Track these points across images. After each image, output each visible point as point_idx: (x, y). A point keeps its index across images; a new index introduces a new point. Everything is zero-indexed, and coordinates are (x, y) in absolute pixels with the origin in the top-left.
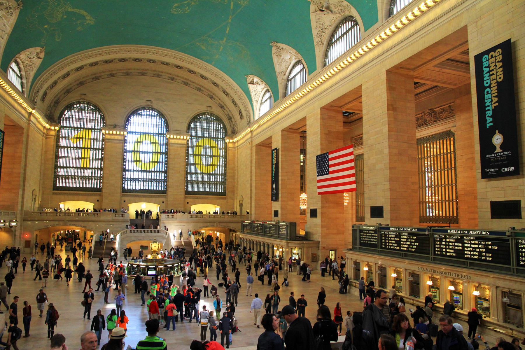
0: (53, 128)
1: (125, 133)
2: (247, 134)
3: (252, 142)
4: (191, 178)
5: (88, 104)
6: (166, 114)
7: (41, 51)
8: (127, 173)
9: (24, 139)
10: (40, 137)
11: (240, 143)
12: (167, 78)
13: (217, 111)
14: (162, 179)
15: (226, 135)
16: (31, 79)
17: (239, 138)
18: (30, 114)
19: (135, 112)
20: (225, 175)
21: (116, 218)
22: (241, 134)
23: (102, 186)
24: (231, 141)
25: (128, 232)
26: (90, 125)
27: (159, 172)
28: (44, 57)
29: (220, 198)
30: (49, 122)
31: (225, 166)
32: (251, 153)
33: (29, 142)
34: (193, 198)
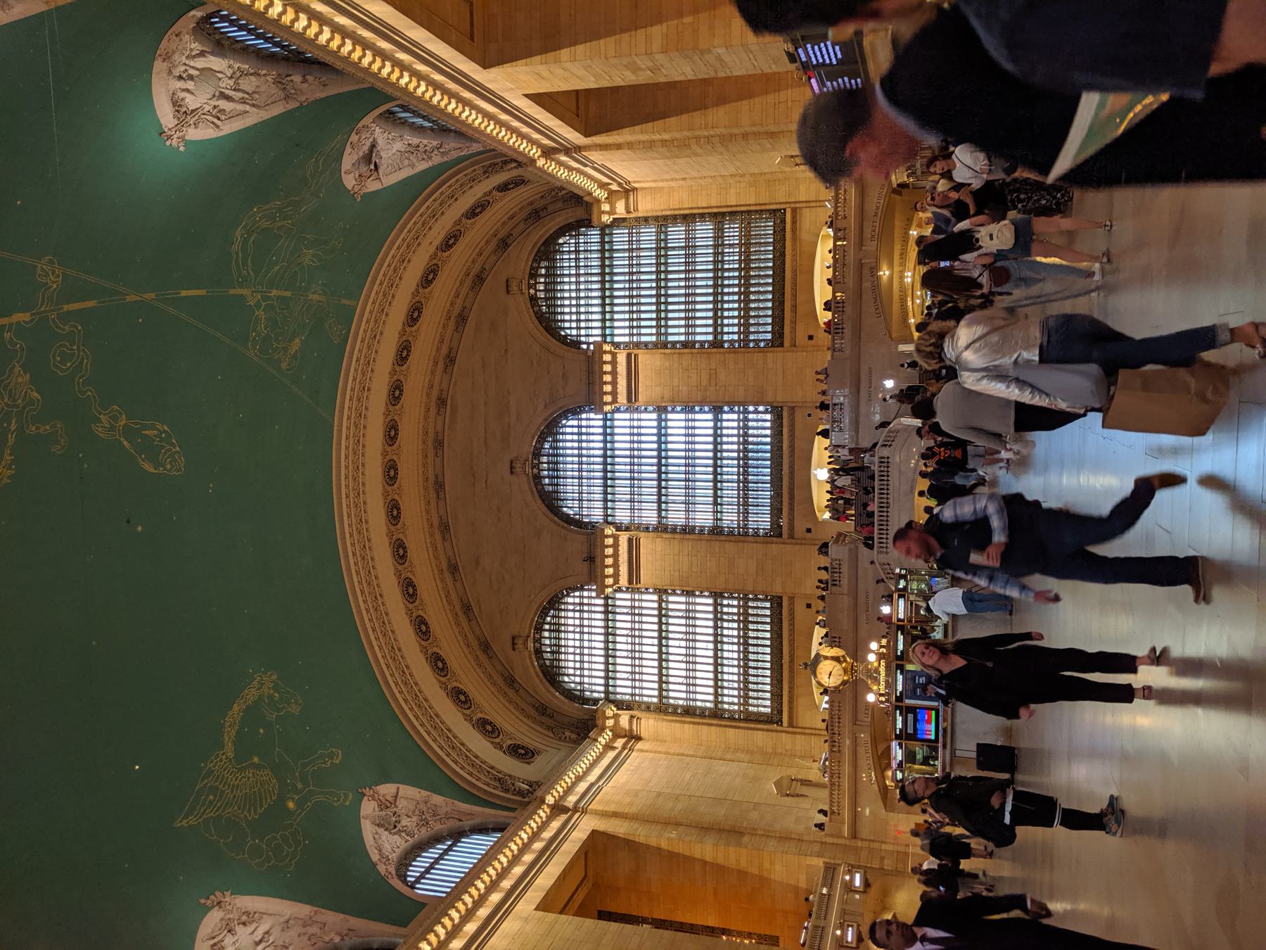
0: (610, 723)
1: (609, 531)
2: (560, 164)
3: (579, 149)
4: (731, 332)
6: (545, 415)
10: (634, 759)
11: (606, 180)
12: (440, 419)
13: (521, 256)
15: (588, 224)
18: (558, 809)
21: (845, 582)
22: (568, 182)
24: (606, 207)
29: (794, 230)
31: (688, 219)
32: (619, 147)
33: (633, 810)
34: (794, 322)
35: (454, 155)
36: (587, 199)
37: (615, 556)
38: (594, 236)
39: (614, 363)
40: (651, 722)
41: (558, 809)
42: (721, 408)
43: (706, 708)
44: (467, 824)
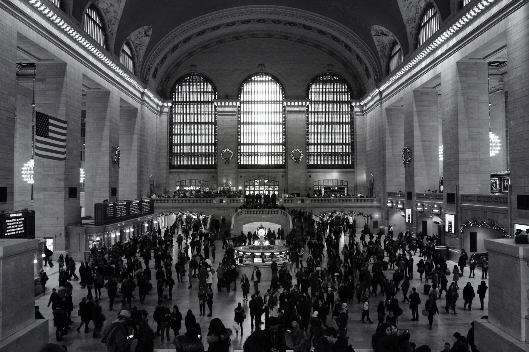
0: (165, 104)
1: (238, 104)
3: (381, 103)
4: (312, 149)
5: (199, 75)
7: (149, 29)
8: (242, 147)
9: (138, 119)
11: (368, 106)
14: (280, 153)
16: (141, 59)
17: (366, 101)
18: (143, 94)
19: (247, 79)
20: (353, 145)
23: (217, 162)
24: (358, 104)
25: (244, 212)
26: (202, 98)
27: (277, 144)
28: (152, 33)
30: (162, 99)
35: (381, 61)
36: (361, 99)
37: (229, 106)
38: (346, 97)
39: (302, 106)
40: (166, 120)
41: (143, 94)
42: (285, 146)
43: (172, 139)
44: (136, 60)
